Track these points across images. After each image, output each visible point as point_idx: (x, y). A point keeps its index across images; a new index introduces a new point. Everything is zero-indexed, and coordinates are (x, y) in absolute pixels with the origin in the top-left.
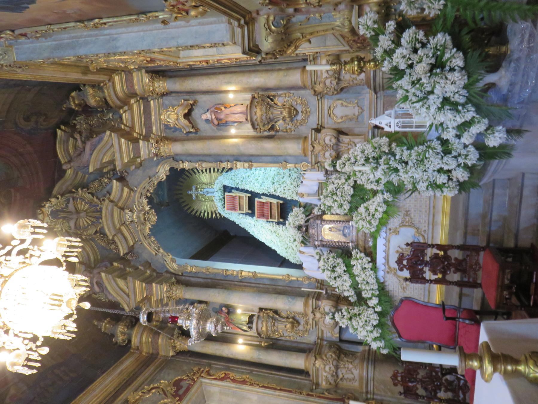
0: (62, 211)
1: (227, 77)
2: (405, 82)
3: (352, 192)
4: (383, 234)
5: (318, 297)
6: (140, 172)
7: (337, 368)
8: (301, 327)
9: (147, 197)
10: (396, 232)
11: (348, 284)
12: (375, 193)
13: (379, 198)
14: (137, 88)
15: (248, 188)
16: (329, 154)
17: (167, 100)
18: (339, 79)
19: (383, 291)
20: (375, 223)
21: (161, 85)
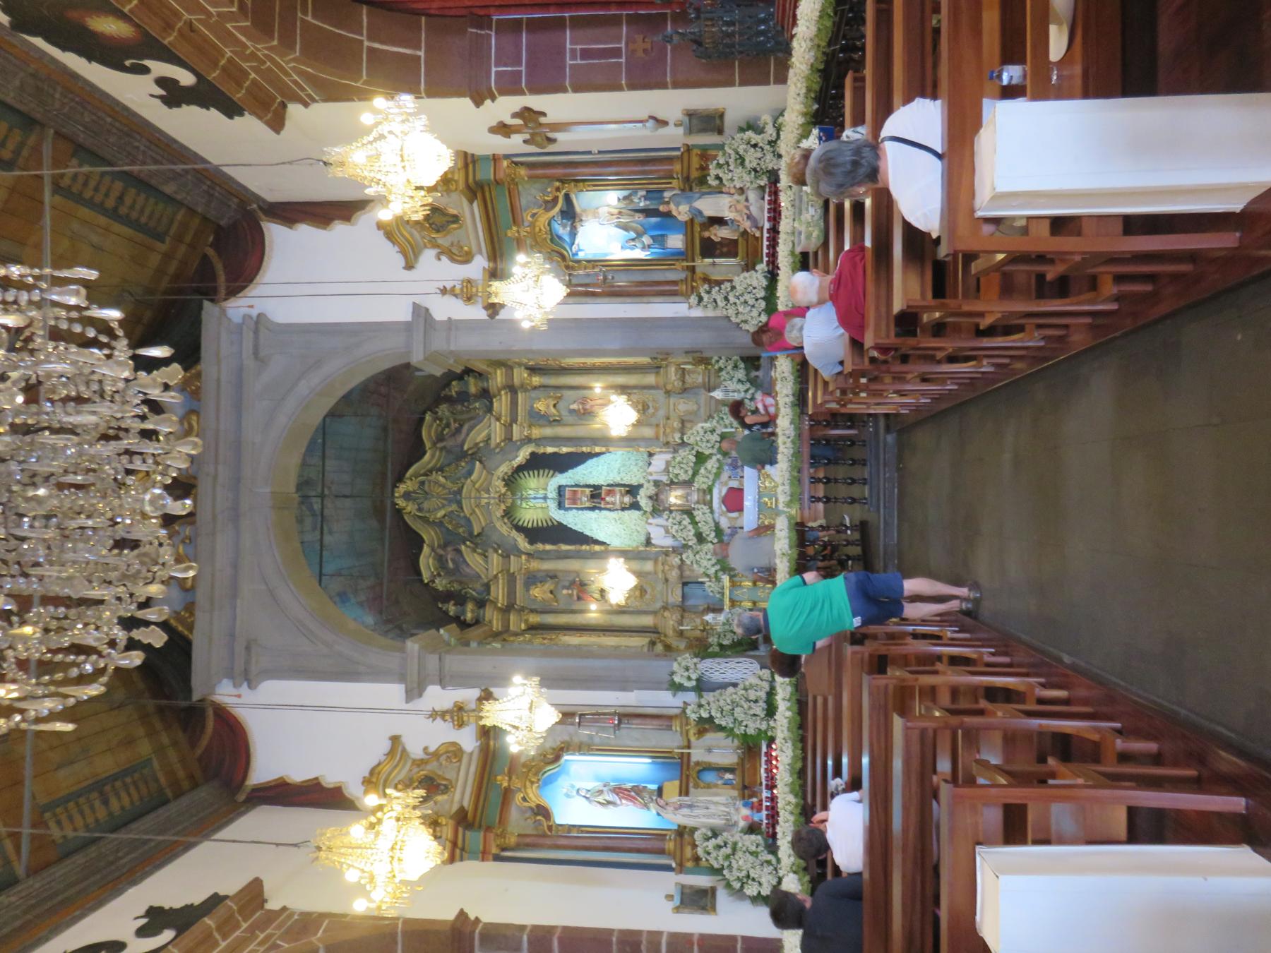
0: (414, 492)
1: (595, 377)
2: (723, 373)
3: (694, 459)
4: (717, 485)
5: (667, 554)
6: (499, 457)
7: (682, 617)
8: (648, 596)
9: (504, 480)
10: (726, 484)
11: (693, 532)
12: (710, 456)
13: (714, 458)
14: (517, 381)
15: (591, 482)
16: (677, 436)
17: (534, 394)
18: (684, 382)
19: (718, 531)
20: (711, 477)
21: (536, 380)
